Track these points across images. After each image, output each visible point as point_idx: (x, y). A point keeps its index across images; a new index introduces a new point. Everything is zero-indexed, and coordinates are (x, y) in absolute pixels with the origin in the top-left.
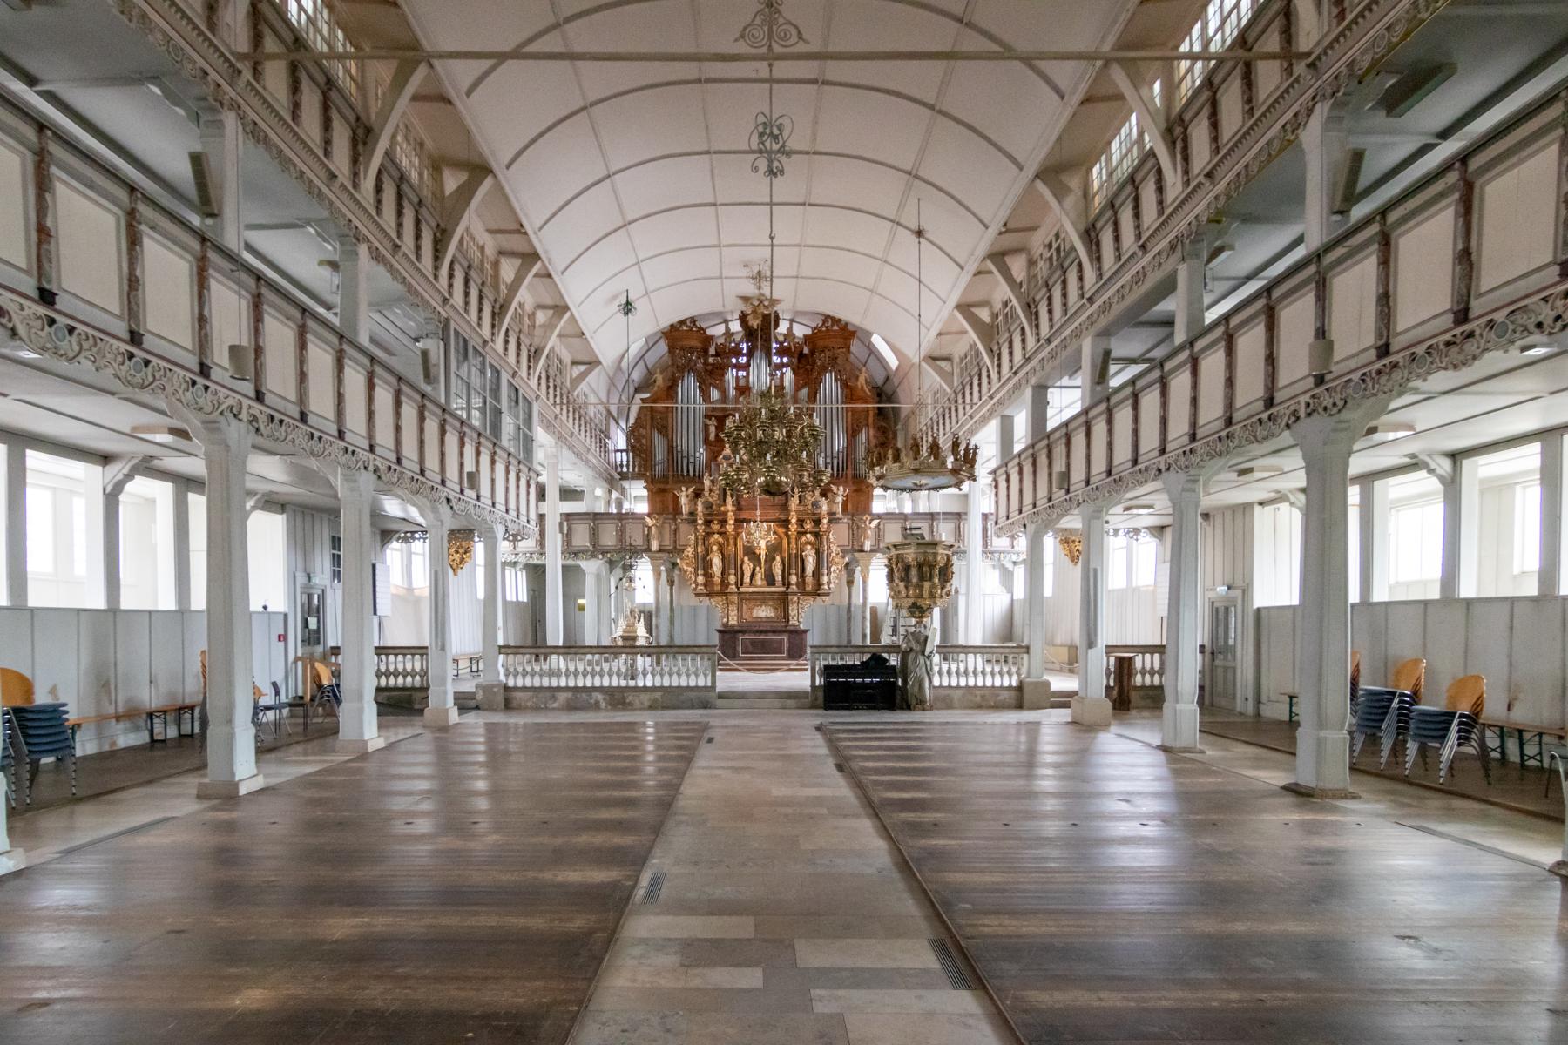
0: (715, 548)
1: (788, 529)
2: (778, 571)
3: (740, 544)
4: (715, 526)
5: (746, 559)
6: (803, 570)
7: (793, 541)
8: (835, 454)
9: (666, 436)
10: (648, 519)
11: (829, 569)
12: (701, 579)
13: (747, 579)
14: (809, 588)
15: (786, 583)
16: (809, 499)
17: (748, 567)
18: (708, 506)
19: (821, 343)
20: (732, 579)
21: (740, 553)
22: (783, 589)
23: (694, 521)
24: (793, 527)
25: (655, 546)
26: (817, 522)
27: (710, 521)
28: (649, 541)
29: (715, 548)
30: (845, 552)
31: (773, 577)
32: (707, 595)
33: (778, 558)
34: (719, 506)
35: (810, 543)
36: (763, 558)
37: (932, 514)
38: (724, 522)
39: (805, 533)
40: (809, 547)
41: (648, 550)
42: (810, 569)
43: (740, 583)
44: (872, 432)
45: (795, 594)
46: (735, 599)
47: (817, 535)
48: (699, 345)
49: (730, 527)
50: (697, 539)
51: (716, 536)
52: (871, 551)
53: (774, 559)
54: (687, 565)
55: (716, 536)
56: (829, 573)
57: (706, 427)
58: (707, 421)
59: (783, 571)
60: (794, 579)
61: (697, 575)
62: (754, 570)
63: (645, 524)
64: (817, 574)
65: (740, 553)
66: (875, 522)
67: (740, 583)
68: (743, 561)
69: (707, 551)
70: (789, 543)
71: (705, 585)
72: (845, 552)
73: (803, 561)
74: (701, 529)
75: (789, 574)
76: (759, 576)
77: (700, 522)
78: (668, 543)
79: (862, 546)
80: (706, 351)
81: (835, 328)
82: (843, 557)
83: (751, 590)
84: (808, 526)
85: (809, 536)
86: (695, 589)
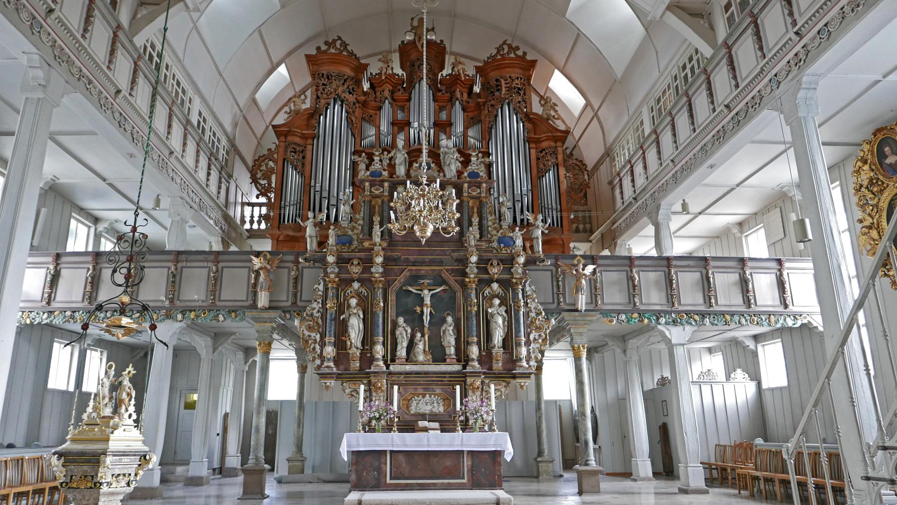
0: (354, 302)
1: (465, 274)
2: (450, 340)
3: (392, 298)
4: (355, 269)
5: (401, 320)
6: (489, 336)
7: (473, 295)
8: (518, 198)
9: (302, 174)
10: (256, 260)
11: (528, 335)
12: (330, 351)
13: (402, 352)
14: (498, 366)
15: (463, 358)
16: (496, 235)
17: (403, 333)
18: (344, 241)
19: (494, 75)
20: (379, 350)
21: (392, 312)
22: (457, 368)
23: (323, 261)
24: (472, 271)
25: (263, 300)
26: (509, 262)
27: (349, 261)
28: (255, 294)
29: (354, 302)
30: (549, 313)
31: (443, 348)
32: (338, 377)
33: (450, 319)
34: (361, 242)
35: (497, 296)
36: (426, 319)
37: (668, 259)
38: (368, 262)
39: (489, 282)
40: (497, 302)
41: (254, 306)
42: (498, 336)
43: (391, 358)
44: (562, 171)
45: (475, 374)
46: (383, 382)
47: (506, 284)
48: (352, 74)
49: (377, 270)
50: (326, 289)
51: (356, 285)
52: (586, 310)
53: (444, 321)
54: (310, 328)
55: (356, 285)
56: (528, 343)
57: (354, 165)
58: (356, 157)
59: (457, 340)
60: (474, 351)
61: (323, 345)
62: (413, 336)
63: (250, 269)
64: (508, 343)
65: (392, 312)
66: (590, 268)
67: (391, 358)
68: (395, 325)
69: (342, 308)
70: (466, 297)
71: (337, 361)
72: (549, 313)
73: (488, 323)
74: (333, 270)
75: (468, 343)
76: (421, 346)
77: (331, 259)
78: (284, 297)
79: (574, 305)
80: (358, 82)
81: (512, 55)
82: (548, 319)
83: (408, 368)
84: (495, 270)
85: (495, 286)
86: (319, 367)
